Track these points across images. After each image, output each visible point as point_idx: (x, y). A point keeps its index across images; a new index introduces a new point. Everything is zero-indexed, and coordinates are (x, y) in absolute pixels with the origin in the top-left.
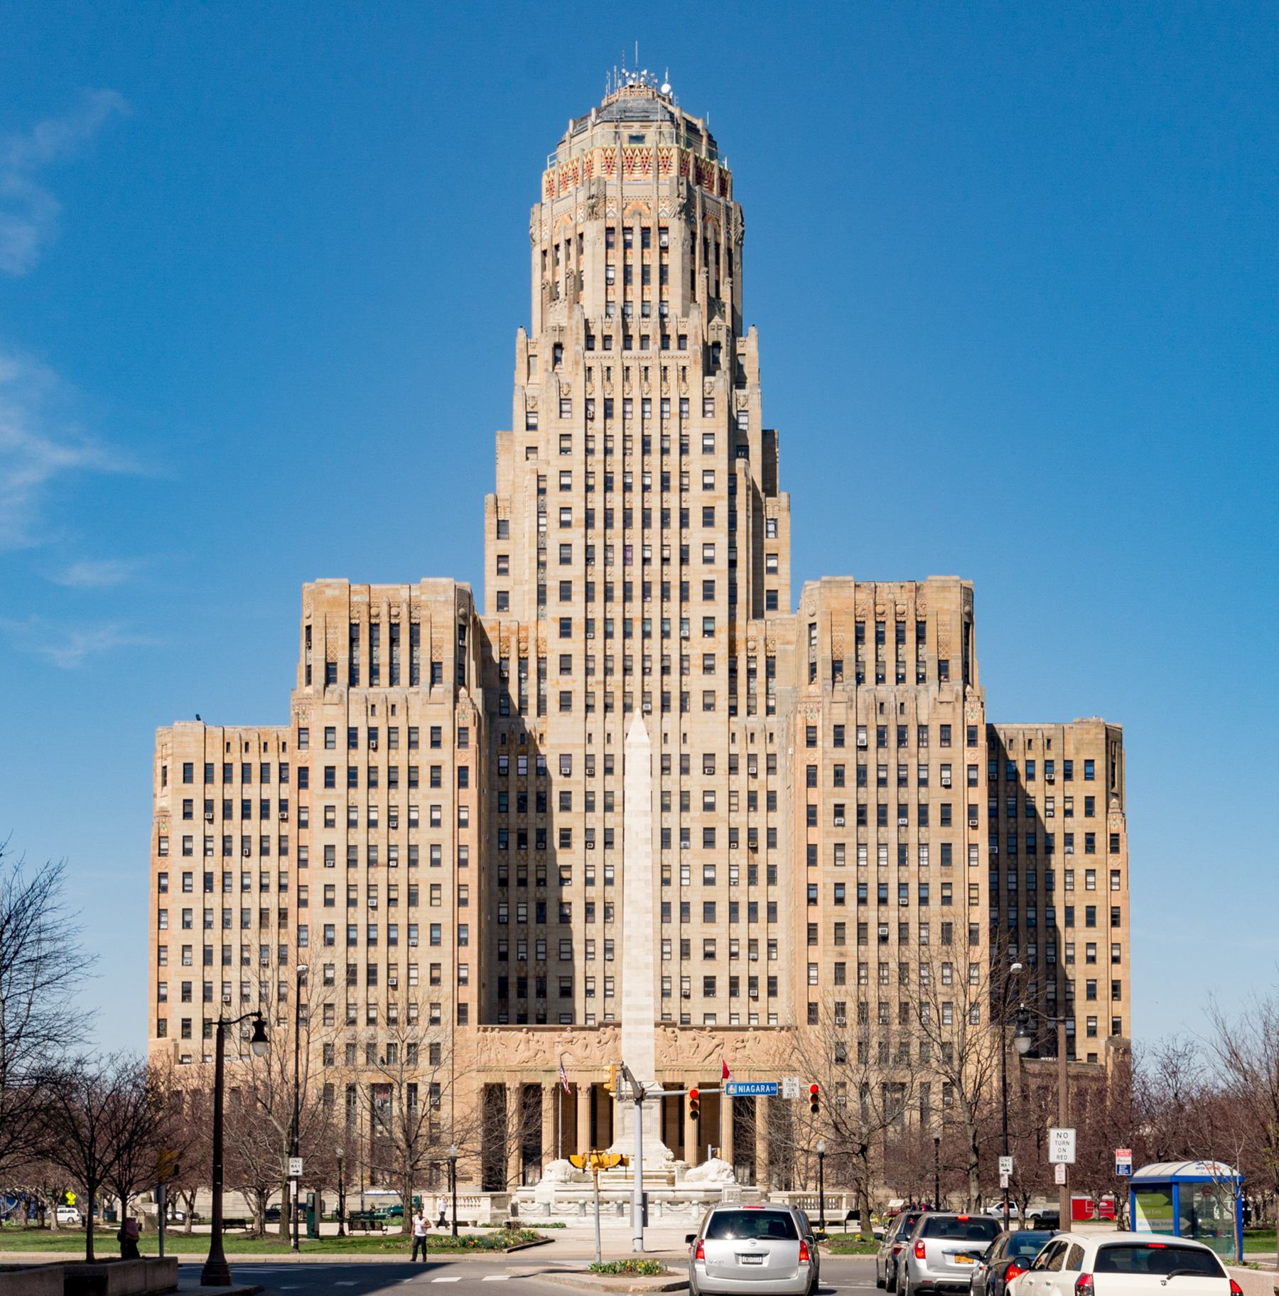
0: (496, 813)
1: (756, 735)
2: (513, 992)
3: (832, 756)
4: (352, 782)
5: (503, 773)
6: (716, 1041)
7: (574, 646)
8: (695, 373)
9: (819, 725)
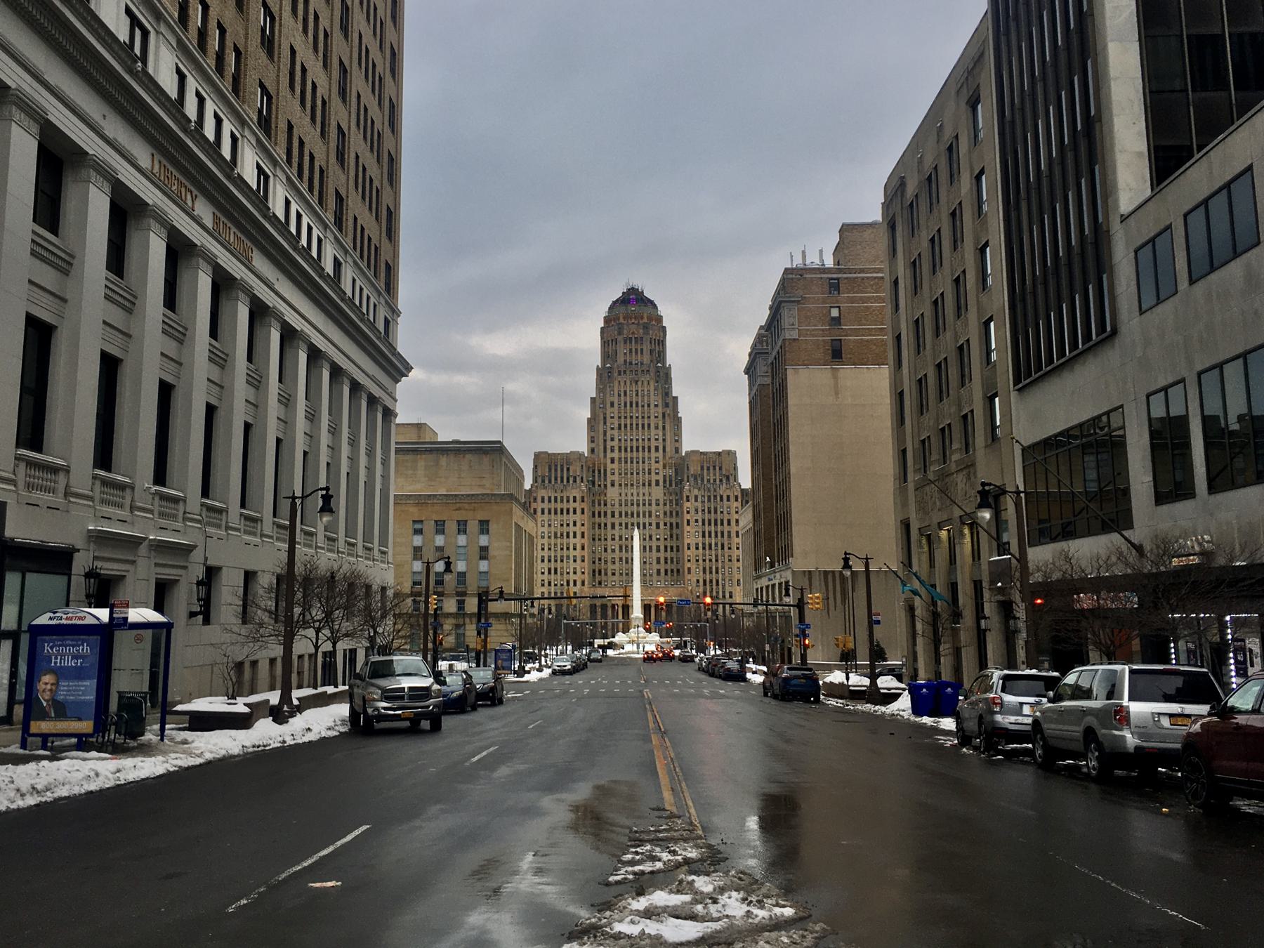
2: (597, 575)
4: (550, 513)
7: (616, 466)
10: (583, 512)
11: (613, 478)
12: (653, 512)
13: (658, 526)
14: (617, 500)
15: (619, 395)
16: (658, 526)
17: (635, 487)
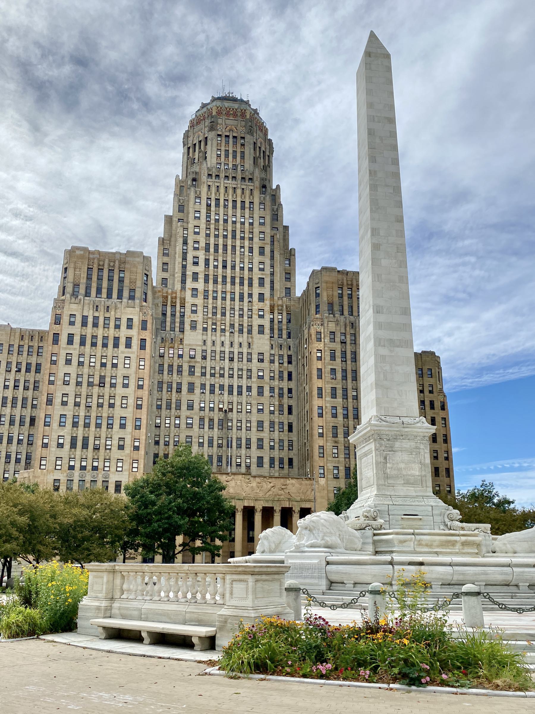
0: (157, 374)
1: (283, 346)
3: (329, 346)
5: (162, 356)
6: (272, 485)
7: (199, 301)
8: (256, 193)
9: (322, 331)
10: (143, 347)
11: (194, 317)
12: (254, 371)
13: (260, 392)
14: (199, 349)
15: (209, 206)
16: (260, 392)
17: (227, 334)
